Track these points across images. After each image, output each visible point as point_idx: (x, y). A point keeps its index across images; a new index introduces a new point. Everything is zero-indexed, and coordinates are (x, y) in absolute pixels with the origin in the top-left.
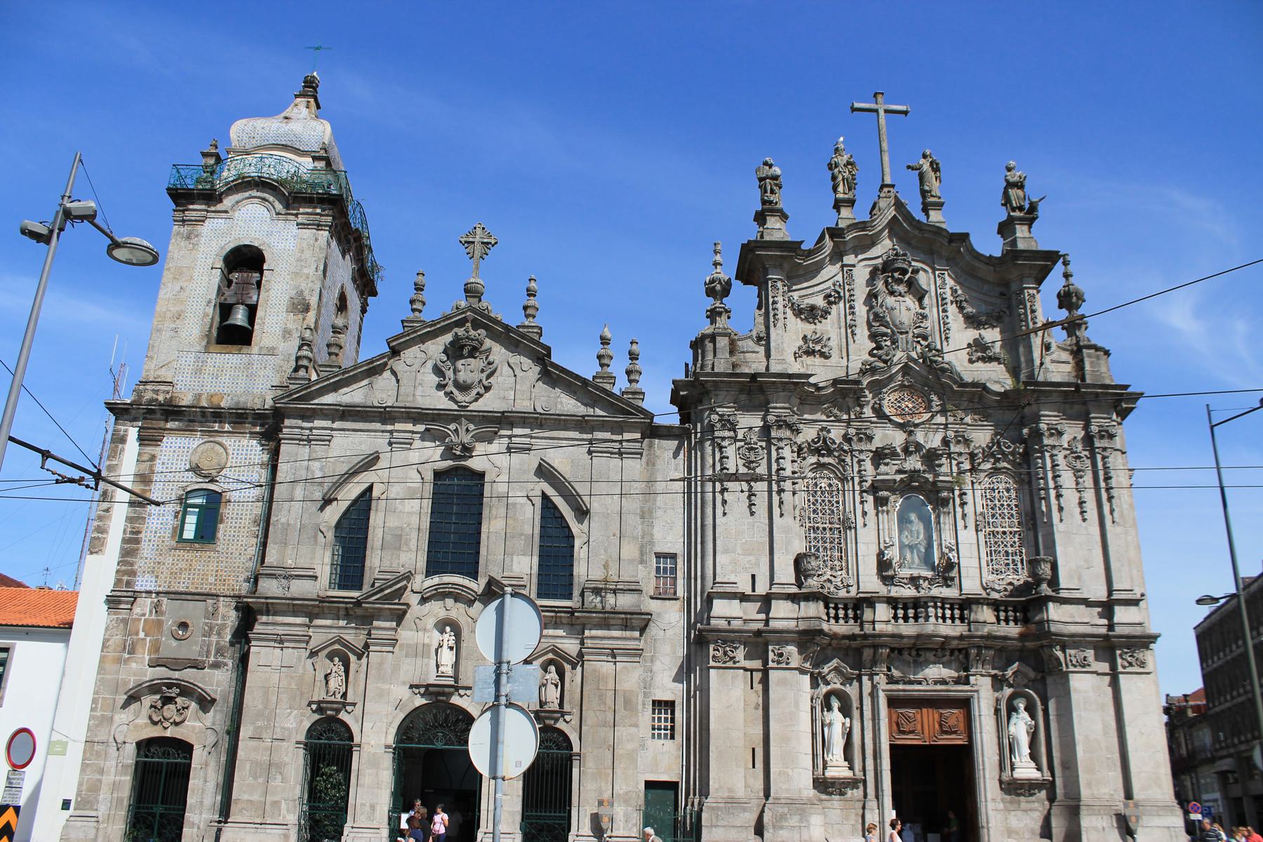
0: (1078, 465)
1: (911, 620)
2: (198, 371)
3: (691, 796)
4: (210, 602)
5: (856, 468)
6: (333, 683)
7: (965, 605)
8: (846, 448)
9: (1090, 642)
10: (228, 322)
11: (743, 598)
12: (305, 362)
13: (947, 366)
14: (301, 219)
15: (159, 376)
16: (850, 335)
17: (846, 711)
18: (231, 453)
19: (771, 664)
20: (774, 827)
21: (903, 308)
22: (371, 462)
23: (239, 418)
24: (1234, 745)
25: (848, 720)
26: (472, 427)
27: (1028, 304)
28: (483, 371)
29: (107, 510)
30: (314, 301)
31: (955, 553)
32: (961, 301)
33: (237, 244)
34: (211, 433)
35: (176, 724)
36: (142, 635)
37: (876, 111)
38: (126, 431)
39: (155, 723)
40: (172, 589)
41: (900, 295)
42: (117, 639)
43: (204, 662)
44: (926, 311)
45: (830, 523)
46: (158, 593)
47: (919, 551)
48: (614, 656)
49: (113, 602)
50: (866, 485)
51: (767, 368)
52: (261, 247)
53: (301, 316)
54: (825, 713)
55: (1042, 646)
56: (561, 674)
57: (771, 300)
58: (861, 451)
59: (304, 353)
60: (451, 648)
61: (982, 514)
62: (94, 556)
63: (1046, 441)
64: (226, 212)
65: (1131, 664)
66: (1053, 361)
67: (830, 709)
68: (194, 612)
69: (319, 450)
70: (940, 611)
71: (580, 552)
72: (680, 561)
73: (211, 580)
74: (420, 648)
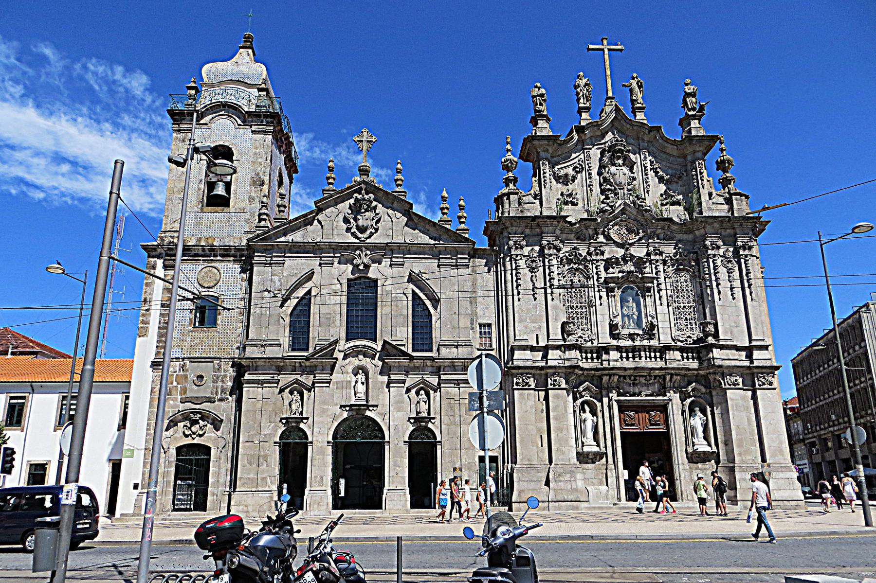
0: (730, 265)
1: (631, 359)
2: (197, 224)
3: (506, 464)
4: (216, 362)
5: (595, 271)
6: (294, 407)
7: (664, 349)
8: (588, 259)
10: (214, 193)
11: (532, 349)
12: (264, 217)
13: (648, 208)
14: (254, 128)
15: (173, 228)
16: (589, 191)
17: (594, 413)
18: (222, 272)
19: (550, 387)
20: (556, 481)
21: (621, 174)
22: (309, 276)
23: (226, 253)
24: (817, 431)
25: (595, 417)
26: (368, 252)
27: (698, 169)
28: (373, 219)
29: (147, 310)
30: (266, 179)
31: (655, 319)
32: (656, 168)
35: (200, 436)
36: (175, 384)
37: (603, 50)
38: (155, 262)
39: (186, 436)
40: (192, 356)
41: (619, 165)
43: (215, 398)
44: (635, 175)
45: (581, 303)
46: (183, 359)
47: (633, 319)
48: (458, 384)
49: (155, 365)
50: (602, 280)
51: (541, 213)
52: (231, 146)
53: (259, 189)
54: (582, 414)
55: (710, 373)
56: (428, 395)
57: (542, 172)
58: (597, 261)
59: (264, 211)
60: (363, 383)
61: (670, 296)
62: (142, 338)
63: (710, 252)
64: (206, 124)
65: (764, 384)
66: (714, 203)
67: (584, 412)
68: (206, 368)
69: (277, 269)
70: (648, 354)
71: (436, 324)
72: (493, 328)
73: (216, 349)
74: (345, 384)
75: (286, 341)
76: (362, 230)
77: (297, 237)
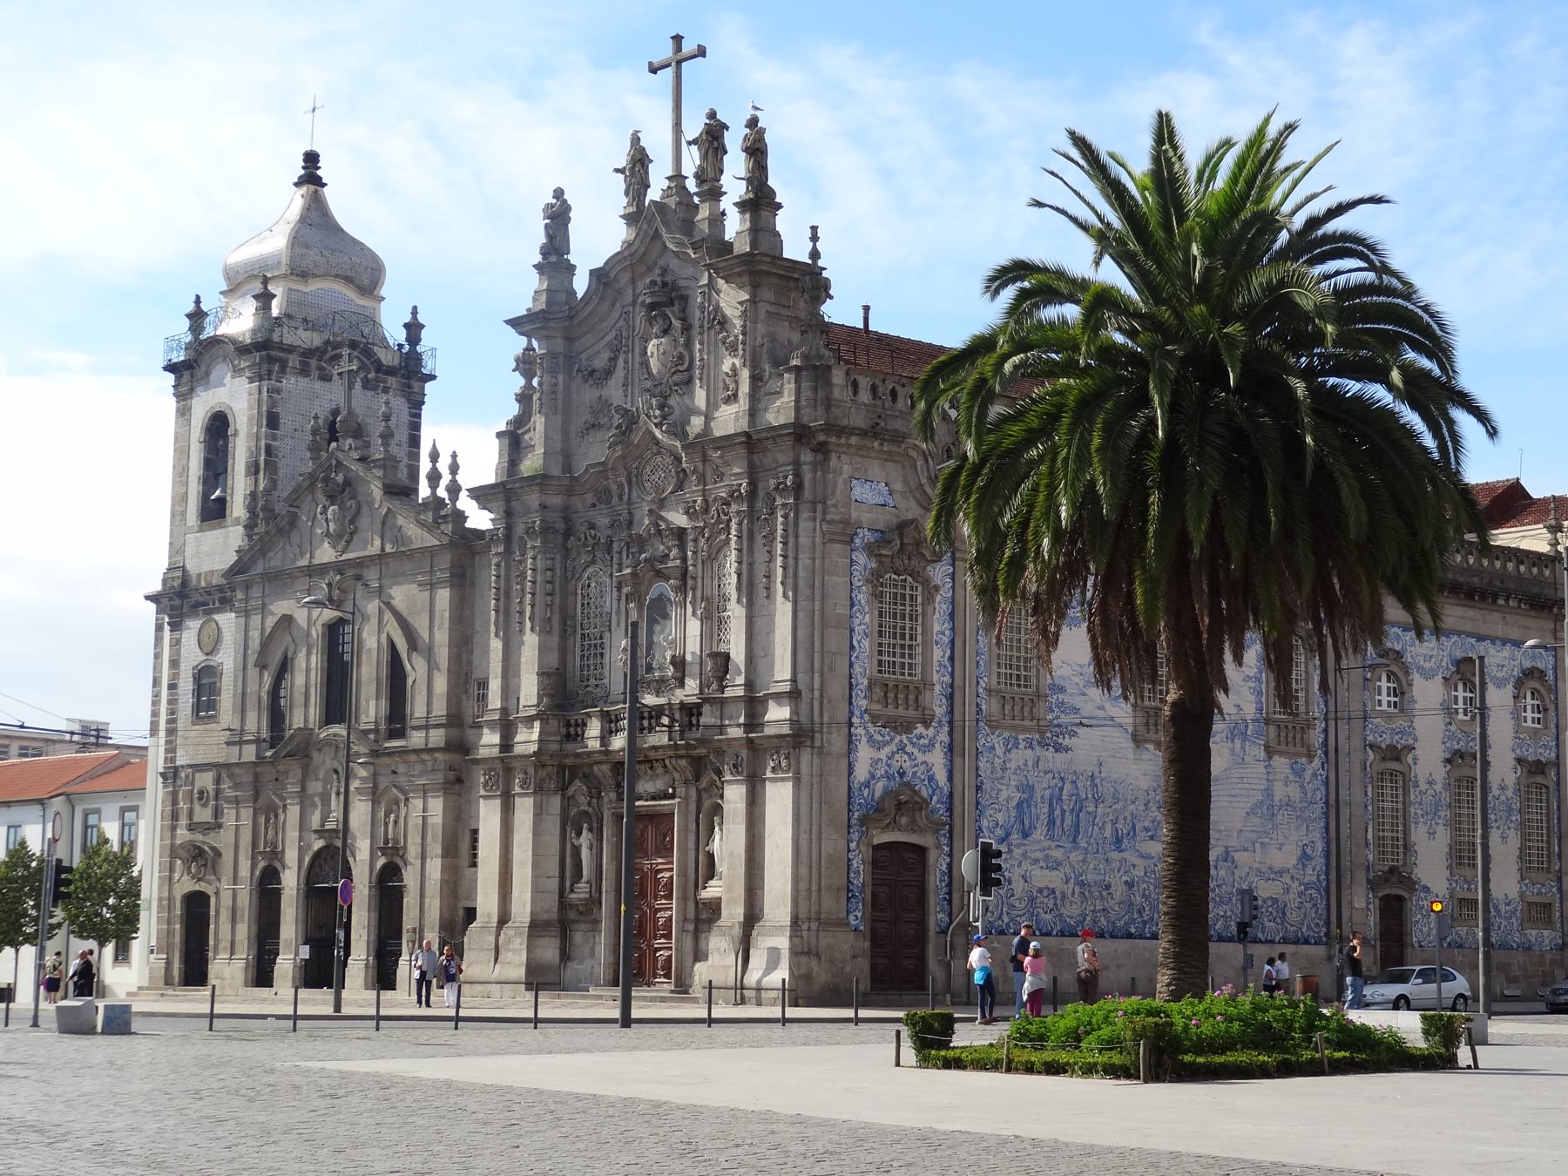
2: (197, 554)
17: (590, 830)
29: (156, 696)
33: (209, 414)
34: (209, 612)
40: (194, 762)
49: (163, 775)
52: (227, 411)
66: (766, 394)
77: (276, 560)
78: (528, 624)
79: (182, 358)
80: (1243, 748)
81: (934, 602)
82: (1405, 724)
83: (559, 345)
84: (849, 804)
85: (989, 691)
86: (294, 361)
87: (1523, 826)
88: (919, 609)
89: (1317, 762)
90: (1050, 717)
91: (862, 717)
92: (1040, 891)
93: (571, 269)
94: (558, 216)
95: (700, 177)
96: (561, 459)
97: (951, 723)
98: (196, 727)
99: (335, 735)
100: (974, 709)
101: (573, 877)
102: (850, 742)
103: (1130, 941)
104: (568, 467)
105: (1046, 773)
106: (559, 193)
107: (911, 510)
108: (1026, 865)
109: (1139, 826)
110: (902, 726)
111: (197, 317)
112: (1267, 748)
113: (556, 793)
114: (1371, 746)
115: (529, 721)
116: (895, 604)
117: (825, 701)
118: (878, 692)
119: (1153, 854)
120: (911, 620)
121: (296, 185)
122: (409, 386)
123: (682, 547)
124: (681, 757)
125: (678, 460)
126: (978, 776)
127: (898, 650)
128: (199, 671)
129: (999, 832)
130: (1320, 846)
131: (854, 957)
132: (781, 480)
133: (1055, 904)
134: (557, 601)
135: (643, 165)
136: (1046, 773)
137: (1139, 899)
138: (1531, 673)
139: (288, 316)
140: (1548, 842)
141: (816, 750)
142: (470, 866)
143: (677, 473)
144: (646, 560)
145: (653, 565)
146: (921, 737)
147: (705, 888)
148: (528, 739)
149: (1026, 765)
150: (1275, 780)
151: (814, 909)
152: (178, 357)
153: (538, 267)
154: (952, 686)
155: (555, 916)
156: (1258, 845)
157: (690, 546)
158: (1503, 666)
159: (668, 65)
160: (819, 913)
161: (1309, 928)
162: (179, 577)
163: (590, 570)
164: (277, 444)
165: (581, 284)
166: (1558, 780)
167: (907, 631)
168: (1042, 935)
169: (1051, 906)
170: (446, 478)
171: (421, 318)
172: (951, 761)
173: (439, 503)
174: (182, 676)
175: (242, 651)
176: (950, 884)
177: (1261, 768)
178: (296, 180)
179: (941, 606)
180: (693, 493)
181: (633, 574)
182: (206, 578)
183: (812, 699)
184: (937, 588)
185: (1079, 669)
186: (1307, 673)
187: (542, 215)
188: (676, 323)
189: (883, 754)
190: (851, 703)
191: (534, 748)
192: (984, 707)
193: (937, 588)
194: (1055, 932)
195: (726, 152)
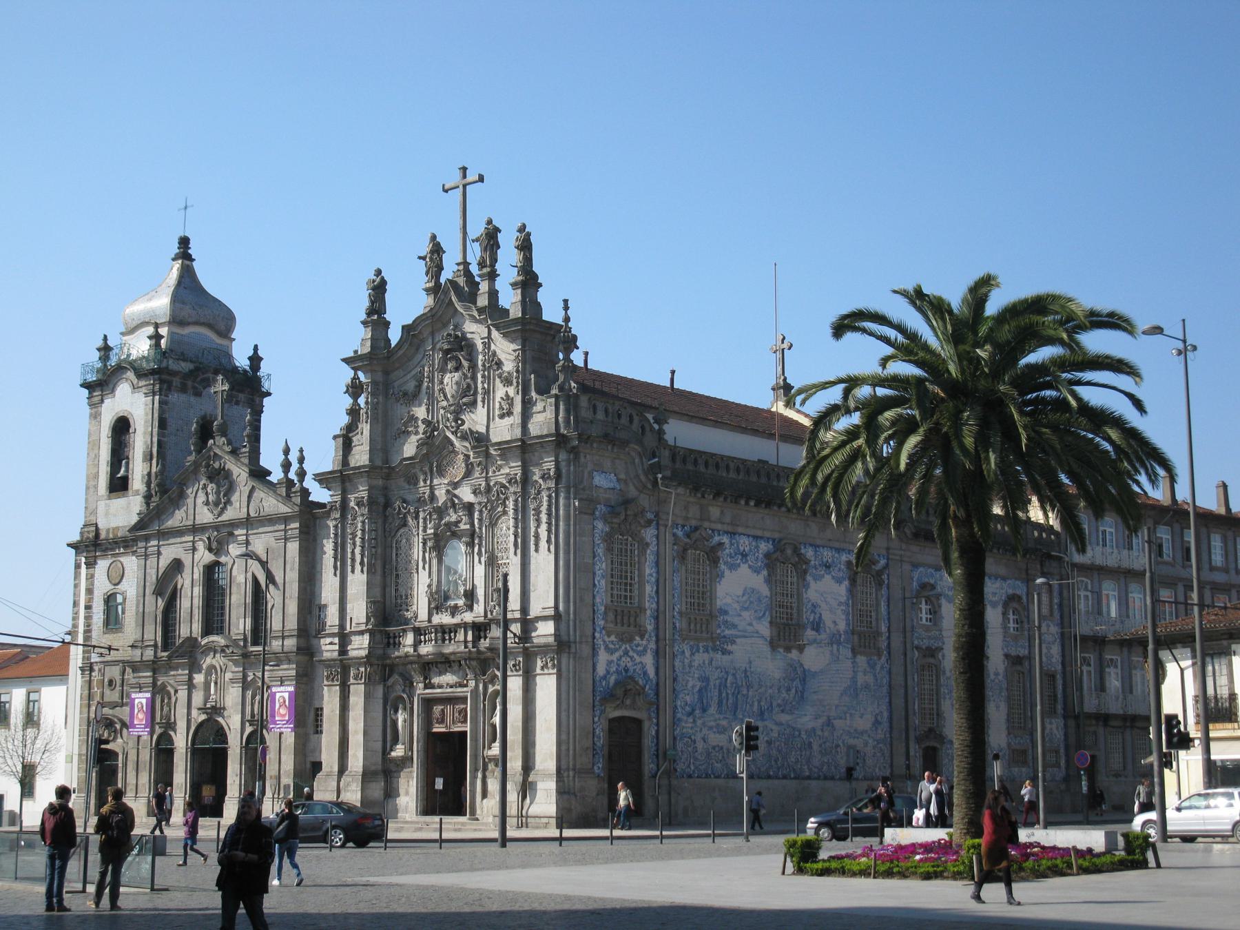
2: (107, 514)
9: (519, 652)
17: (405, 709)
33: (115, 418)
36: (96, 689)
42: (86, 692)
49: (82, 669)
75: (159, 640)
76: (216, 504)
78: (358, 567)
79: (95, 379)
80: (838, 650)
81: (646, 552)
82: (937, 633)
83: (379, 377)
84: (593, 691)
85: (680, 613)
86: (176, 381)
87: (1009, 699)
88: (636, 559)
89: (883, 659)
90: (718, 631)
91: (601, 633)
92: (714, 748)
93: (387, 324)
94: (379, 289)
95: (482, 265)
96: (381, 454)
97: (657, 636)
98: (107, 636)
99: (213, 642)
100: (671, 624)
101: (392, 740)
102: (594, 649)
103: (770, 781)
104: (386, 461)
105: (717, 668)
106: (379, 272)
107: (632, 492)
108: (705, 731)
109: (775, 704)
110: (625, 639)
111: (105, 349)
112: (853, 650)
113: (380, 683)
114: (917, 648)
115: (361, 633)
116: (621, 556)
117: (577, 622)
118: (611, 616)
119: (784, 722)
120: (631, 566)
121: (174, 260)
122: (253, 400)
123: (471, 515)
124: (473, 659)
125: (467, 457)
126: (674, 671)
127: (623, 587)
128: (109, 597)
129: (688, 709)
130: (886, 714)
131: (598, 795)
132: (546, 472)
133: (723, 757)
134: (379, 551)
135: (439, 255)
136: (717, 668)
137: (774, 751)
138: (1012, 598)
139: (171, 350)
140: (1024, 710)
141: (571, 655)
142: (314, 733)
143: (467, 465)
144: (445, 525)
145: (450, 528)
146: (638, 645)
147: (490, 748)
148: (360, 646)
149: (704, 663)
150: (858, 671)
151: (571, 763)
152: (92, 378)
153: (364, 323)
154: (657, 611)
155: (380, 767)
156: (848, 715)
157: (476, 515)
158: (996, 593)
159: (458, 187)
160: (574, 765)
161: (880, 769)
162: (93, 531)
163: (402, 531)
164: (165, 439)
165: (395, 335)
166: (1030, 668)
167: (629, 574)
168: (716, 777)
169: (720, 758)
170: (295, 466)
171: (260, 353)
172: (657, 662)
173: (290, 483)
174: (96, 599)
175: (142, 583)
176: (657, 744)
177: (849, 663)
178: (173, 256)
179: (650, 557)
180: (478, 478)
181: (435, 534)
182: (113, 533)
183: (569, 621)
184: (647, 545)
185: (737, 599)
186: (877, 598)
187: (366, 287)
188: (465, 364)
189: (615, 657)
190: (594, 623)
191: (364, 653)
192: (677, 625)
193: (647, 545)
194: (723, 776)
195: (498, 247)
